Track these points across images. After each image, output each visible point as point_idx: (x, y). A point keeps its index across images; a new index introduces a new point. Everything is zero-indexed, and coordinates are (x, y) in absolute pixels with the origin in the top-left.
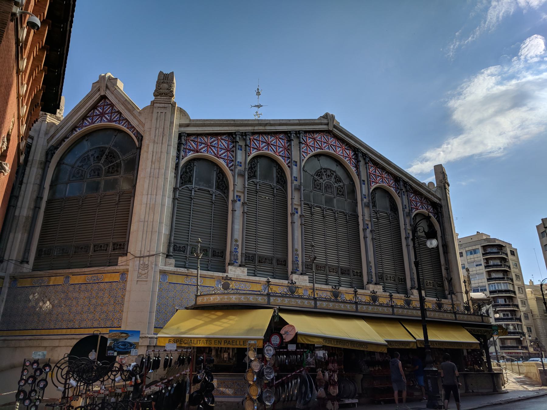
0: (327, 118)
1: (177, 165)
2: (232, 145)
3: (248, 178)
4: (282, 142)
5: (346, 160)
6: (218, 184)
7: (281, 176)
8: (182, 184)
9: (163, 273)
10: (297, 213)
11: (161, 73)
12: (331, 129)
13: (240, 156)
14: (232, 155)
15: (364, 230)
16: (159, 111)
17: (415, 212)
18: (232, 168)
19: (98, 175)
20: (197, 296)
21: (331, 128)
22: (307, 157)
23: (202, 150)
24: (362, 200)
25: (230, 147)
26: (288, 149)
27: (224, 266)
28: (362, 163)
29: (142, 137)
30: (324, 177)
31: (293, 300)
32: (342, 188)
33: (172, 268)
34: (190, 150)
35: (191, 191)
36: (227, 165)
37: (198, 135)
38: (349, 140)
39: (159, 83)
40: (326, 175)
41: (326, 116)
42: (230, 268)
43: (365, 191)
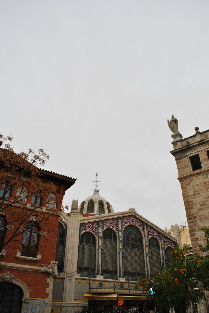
1: (79, 235)
4: (115, 222)
8: (81, 243)
9: (76, 279)
11: (73, 200)
15: (146, 257)
17: (166, 247)
20: (89, 289)
21: (133, 214)
22: (124, 227)
23: (87, 229)
24: (145, 244)
26: (117, 225)
28: (145, 228)
29: (67, 225)
30: (131, 235)
31: (122, 290)
33: (78, 277)
37: (86, 223)
38: (141, 218)
42: (98, 276)
43: (146, 240)
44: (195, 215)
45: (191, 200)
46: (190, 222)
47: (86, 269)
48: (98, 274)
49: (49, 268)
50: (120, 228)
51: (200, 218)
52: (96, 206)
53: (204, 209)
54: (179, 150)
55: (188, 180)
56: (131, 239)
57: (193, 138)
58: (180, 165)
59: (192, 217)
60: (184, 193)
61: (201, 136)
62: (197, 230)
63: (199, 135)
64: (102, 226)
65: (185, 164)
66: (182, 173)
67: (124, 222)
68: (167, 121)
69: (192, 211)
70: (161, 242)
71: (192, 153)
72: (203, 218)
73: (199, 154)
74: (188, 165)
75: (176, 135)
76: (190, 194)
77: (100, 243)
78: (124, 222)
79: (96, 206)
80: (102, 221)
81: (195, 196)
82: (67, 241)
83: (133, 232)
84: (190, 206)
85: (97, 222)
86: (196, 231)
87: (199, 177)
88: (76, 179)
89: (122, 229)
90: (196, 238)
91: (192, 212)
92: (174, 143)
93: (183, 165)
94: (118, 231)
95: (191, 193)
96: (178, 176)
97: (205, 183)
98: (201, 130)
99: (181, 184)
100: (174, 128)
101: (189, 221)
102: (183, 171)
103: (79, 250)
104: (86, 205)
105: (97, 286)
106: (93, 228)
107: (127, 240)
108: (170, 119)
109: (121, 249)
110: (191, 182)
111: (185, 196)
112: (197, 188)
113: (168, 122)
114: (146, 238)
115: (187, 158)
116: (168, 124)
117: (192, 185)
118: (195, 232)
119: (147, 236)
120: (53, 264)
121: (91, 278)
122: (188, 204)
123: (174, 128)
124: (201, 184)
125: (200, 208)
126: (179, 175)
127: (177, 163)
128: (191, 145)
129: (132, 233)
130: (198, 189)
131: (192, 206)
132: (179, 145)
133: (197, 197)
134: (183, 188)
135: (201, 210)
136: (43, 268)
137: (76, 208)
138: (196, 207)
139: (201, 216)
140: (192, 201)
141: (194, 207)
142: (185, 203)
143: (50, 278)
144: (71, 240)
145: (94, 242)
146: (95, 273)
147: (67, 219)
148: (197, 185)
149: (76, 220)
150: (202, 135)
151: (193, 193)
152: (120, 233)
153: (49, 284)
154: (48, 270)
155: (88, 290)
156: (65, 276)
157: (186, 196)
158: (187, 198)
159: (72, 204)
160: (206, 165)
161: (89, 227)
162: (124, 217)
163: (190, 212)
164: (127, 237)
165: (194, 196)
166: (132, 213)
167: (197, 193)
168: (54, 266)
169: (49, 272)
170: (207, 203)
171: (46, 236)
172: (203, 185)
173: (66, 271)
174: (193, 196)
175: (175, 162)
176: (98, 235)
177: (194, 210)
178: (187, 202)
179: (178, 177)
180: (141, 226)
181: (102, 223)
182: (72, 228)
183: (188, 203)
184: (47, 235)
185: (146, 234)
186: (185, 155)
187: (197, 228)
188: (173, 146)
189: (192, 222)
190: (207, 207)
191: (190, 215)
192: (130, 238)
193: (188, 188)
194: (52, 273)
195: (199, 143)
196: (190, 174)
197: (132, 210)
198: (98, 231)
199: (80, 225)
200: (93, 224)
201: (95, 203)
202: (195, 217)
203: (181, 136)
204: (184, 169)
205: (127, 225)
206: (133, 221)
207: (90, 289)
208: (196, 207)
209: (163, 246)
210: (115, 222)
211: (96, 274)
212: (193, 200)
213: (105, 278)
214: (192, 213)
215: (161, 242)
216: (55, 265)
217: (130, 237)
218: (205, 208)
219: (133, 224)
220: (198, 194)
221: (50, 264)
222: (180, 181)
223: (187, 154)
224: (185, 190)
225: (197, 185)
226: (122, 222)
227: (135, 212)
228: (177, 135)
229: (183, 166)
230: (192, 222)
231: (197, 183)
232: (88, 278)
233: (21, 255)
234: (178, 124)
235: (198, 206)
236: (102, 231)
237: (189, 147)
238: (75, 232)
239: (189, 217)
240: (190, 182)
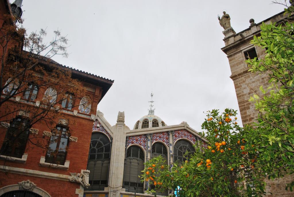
0: (184, 124)
1: (126, 149)
2: (146, 139)
4: (165, 136)
5: (192, 142)
8: (127, 157)
9: (121, 194)
10: (172, 166)
11: (119, 112)
13: (149, 144)
14: (146, 143)
16: (119, 128)
19: (95, 152)
21: (185, 128)
22: (176, 141)
23: (134, 143)
25: (145, 140)
26: (168, 139)
27: (143, 191)
29: (112, 138)
30: (183, 150)
33: (124, 192)
34: (130, 143)
35: (130, 159)
36: (144, 148)
37: (133, 136)
38: (193, 132)
39: (119, 117)
40: (184, 148)
41: (183, 123)
44: (252, 116)
45: (247, 99)
47: (133, 184)
48: (146, 190)
49: (79, 176)
50: (171, 142)
54: (231, 46)
55: (243, 78)
57: (247, 32)
58: (233, 62)
59: (248, 118)
60: (238, 92)
61: (257, 28)
63: (255, 26)
64: (151, 139)
65: (239, 61)
66: (235, 71)
67: (176, 136)
68: (218, 18)
71: (245, 48)
73: (255, 48)
75: (228, 30)
76: (245, 93)
77: (149, 157)
78: (176, 136)
80: (151, 135)
82: (112, 154)
83: (186, 146)
84: (246, 106)
85: (145, 135)
88: (113, 81)
91: (248, 113)
92: (225, 40)
93: (236, 61)
95: (246, 91)
97: (263, 79)
98: (256, 22)
99: (234, 83)
100: (225, 24)
102: (237, 69)
103: (125, 164)
104: (140, 125)
106: (141, 141)
107: (179, 155)
108: (221, 15)
109: (171, 164)
110: (247, 79)
111: (239, 96)
112: (254, 85)
113: (219, 19)
115: (241, 53)
116: (219, 21)
117: (248, 82)
120: (84, 172)
122: (243, 104)
123: (225, 24)
126: (232, 73)
127: (230, 61)
128: (246, 39)
129: (185, 148)
130: (255, 86)
131: (248, 106)
132: (232, 41)
134: (237, 87)
136: (71, 177)
137: (122, 120)
138: (253, 107)
140: (247, 101)
141: (251, 107)
142: (239, 103)
143: (79, 188)
144: (116, 154)
145: (142, 156)
147: (113, 132)
149: (122, 133)
150: (258, 27)
153: (78, 195)
154: (77, 179)
156: (110, 191)
157: (240, 96)
158: (242, 97)
159: (118, 116)
161: (137, 140)
162: (175, 131)
163: (246, 113)
164: (179, 151)
165: (250, 95)
166: (184, 126)
168: (84, 175)
169: (79, 181)
171: (77, 141)
172: (261, 81)
173: (110, 186)
174: (249, 94)
175: (227, 60)
176: (146, 149)
177: (250, 110)
178: (241, 102)
179: (231, 75)
180: (194, 141)
181: (151, 137)
182: (117, 141)
183: (244, 103)
184: (78, 140)
186: (239, 50)
188: (225, 42)
191: (246, 117)
192: (182, 153)
193: (243, 86)
194: (81, 183)
196: (245, 70)
197: (184, 124)
198: (146, 145)
199: (127, 137)
200: (141, 137)
201: (149, 123)
202: (253, 118)
204: (238, 66)
205: (179, 139)
206: (185, 135)
208: (253, 106)
210: (165, 136)
211: (144, 190)
214: (248, 113)
216: (86, 173)
217: (182, 151)
219: (186, 138)
221: (80, 172)
222: (233, 80)
223: (241, 49)
224: (239, 89)
227: (187, 126)
228: (230, 31)
229: (237, 62)
231: (253, 80)
232: (134, 193)
233: (45, 162)
234: (230, 20)
237: (243, 41)
238: (120, 145)
239: (244, 119)
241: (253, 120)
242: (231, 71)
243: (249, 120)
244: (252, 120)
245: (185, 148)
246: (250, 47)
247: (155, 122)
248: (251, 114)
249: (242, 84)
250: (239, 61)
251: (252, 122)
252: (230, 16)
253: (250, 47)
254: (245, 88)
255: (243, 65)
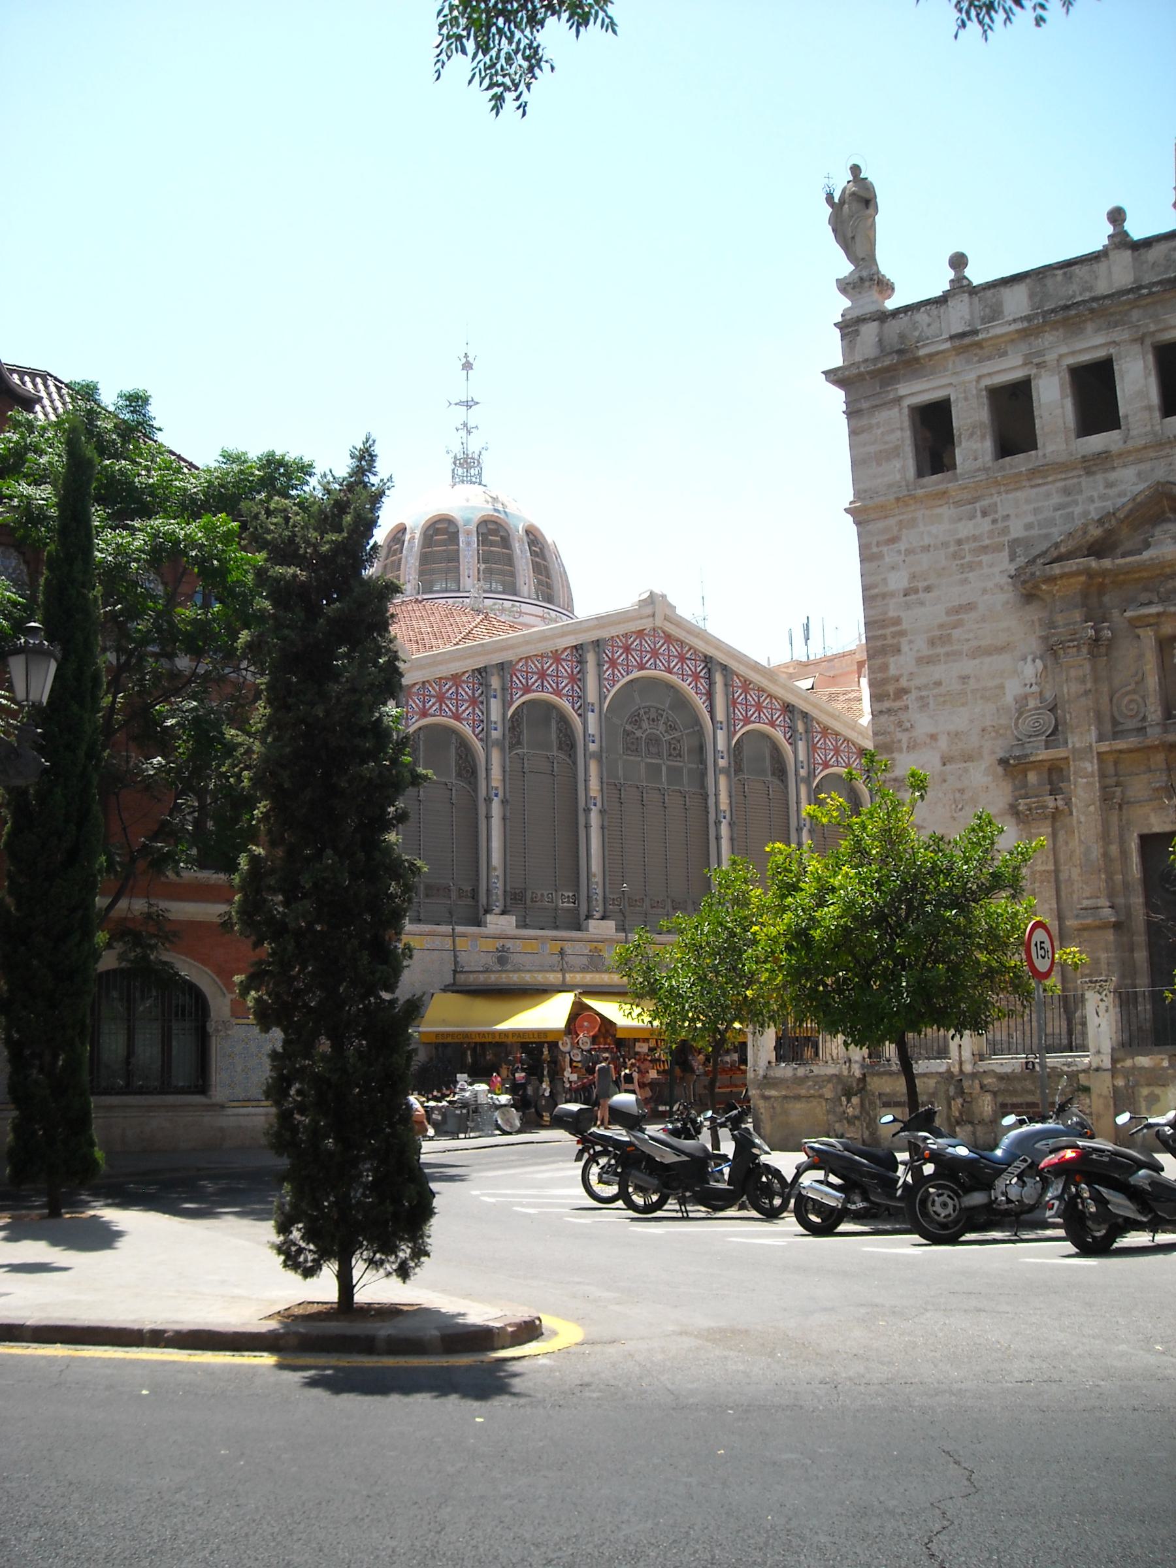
3: (510, 748)
5: (685, 684)
6: (460, 767)
7: (566, 735)
10: (595, 805)
12: (659, 622)
18: (480, 736)
20: (455, 972)
27: (478, 914)
30: (645, 725)
32: (679, 742)
36: (474, 732)
40: (648, 719)
42: (489, 918)
43: (721, 745)
44: (904, 683)
46: (881, 712)
50: (592, 696)
51: (922, 698)
52: (468, 550)
53: (942, 658)
55: (892, 521)
56: (647, 744)
59: (891, 689)
62: (905, 747)
65: (886, 443)
67: (613, 663)
69: (896, 665)
70: (795, 752)
72: (934, 696)
74: (897, 448)
79: (468, 550)
81: (913, 597)
83: (658, 709)
84: (890, 641)
86: (900, 750)
87: (938, 511)
89: (602, 697)
90: (895, 780)
91: (892, 667)
94: (579, 708)
95: (897, 581)
96: (852, 499)
97: (959, 542)
101: (878, 707)
105: (490, 960)
108: (841, 181)
111: (871, 595)
113: (829, 198)
114: (721, 735)
115: (896, 410)
116: (830, 210)
118: (895, 755)
119: (725, 726)
121: (460, 929)
122: (880, 632)
124: (945, 545)
125: (926, 651)
127: (853, 433)
131: (895, 641)
133: (922, 604)
134: (867, 556)
135: (929, 661)
138: (911, 649)
139: (926, 686)
141: (905, 648)
146: (476, 906)
148: (926, 549)
150: (976, 299)
151: (904, 583)
152: (592, 718)
155: (449, 980)
160: (976, 459)
163: (884, 667)
165: (908, 598)
167: (921, 585)
170: (956, 633)
172: (952, 549)
174: (905, 595)
175: (842, 425)
179: (851, 503)
180: (696, 676)
181: (503, 678)
183: (883, 627)
185: (720, 715)
186: (891, 396)
187: (904, 737)
189: (889, 711)
190: (954, 653)
191: (885, 682)
193: (887, 559)
195: (957, 343)
202: (905, 691)
203: (886, 287)
204: (879, 464)
207: (457, 976)
209: (803, 772)
212: (903, 614)
213: (522, 924)
214: (893, 671)
215: (795, 752)
218: (947, 654)
220: (928, 589)
224: (874, 564)
225: (926, 549)
226: (599, 665)
227: (668, 612)
228: (867, 284)
230: (889, 711)
231: (926, 542)
235: (920, 645)
236: (504, 714)
240: (900, 530)
241: (905, 698)
242: (855, 481)
243: (892, 696)
244: (901, 697)
245: (653, 715)
246: (934, 389)
247: (495, 532)
248: (901, 675)
249: (885, 549)
250: (886, 443)
251: (902, 703)
252: (880, 200)
253: (934, 389)
254: (893, 568)
255: (898, 466)
